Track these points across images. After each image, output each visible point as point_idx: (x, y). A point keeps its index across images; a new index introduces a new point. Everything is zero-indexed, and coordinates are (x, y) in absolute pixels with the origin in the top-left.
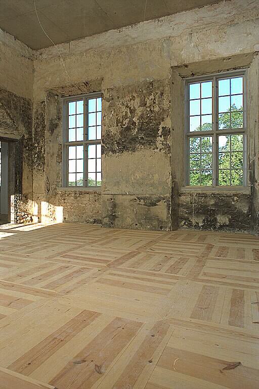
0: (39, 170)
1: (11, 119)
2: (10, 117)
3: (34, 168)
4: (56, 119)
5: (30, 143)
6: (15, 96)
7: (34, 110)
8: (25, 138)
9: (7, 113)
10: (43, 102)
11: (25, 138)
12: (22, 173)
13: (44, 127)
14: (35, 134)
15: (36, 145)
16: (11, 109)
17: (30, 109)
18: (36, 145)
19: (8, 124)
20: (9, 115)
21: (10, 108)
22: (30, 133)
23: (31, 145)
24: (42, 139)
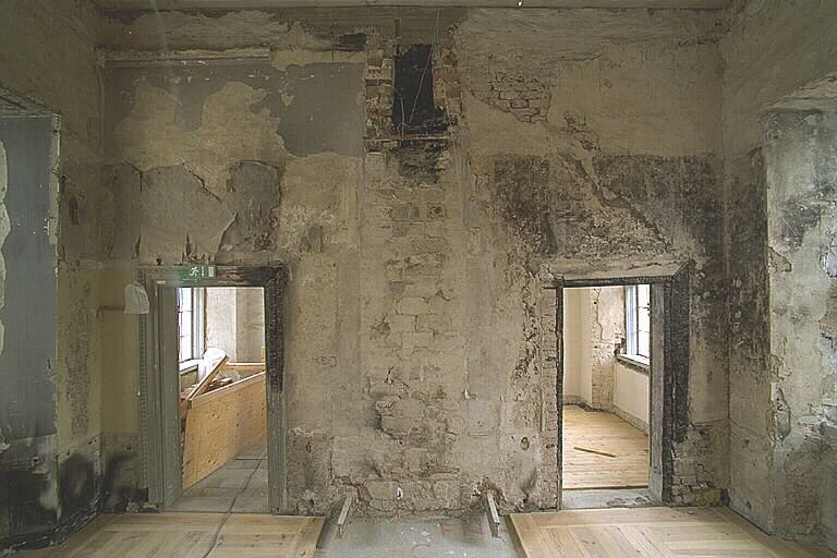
0: (749, 359)
1: (648, 225)
2: (643, 220)
3: (733, 350)
4: (810, 194)
5: (718, 278)
6: (660, 162)
7: (728, 182)
8: (699, 267)
9: (633, 212)
10: (753, 152)
11: (699, 267)
12: (686, 373)
13: (761, 229)
14: (731, 252)
15: (738, 284)
16: (646, 200)
17: (712, 182)
18: (738, 284)
19: (636, 243)
20: (639, 216)
21: (640, 196)
22: (713, 251)
23: (721, 284)
24: (757, 267)
